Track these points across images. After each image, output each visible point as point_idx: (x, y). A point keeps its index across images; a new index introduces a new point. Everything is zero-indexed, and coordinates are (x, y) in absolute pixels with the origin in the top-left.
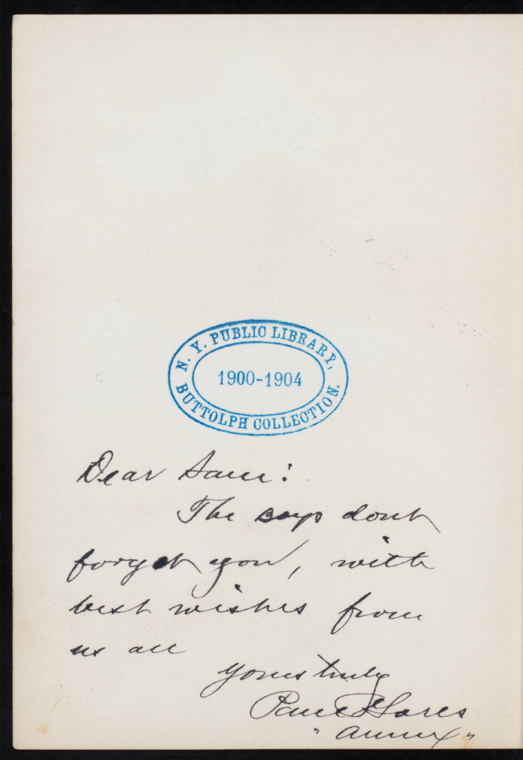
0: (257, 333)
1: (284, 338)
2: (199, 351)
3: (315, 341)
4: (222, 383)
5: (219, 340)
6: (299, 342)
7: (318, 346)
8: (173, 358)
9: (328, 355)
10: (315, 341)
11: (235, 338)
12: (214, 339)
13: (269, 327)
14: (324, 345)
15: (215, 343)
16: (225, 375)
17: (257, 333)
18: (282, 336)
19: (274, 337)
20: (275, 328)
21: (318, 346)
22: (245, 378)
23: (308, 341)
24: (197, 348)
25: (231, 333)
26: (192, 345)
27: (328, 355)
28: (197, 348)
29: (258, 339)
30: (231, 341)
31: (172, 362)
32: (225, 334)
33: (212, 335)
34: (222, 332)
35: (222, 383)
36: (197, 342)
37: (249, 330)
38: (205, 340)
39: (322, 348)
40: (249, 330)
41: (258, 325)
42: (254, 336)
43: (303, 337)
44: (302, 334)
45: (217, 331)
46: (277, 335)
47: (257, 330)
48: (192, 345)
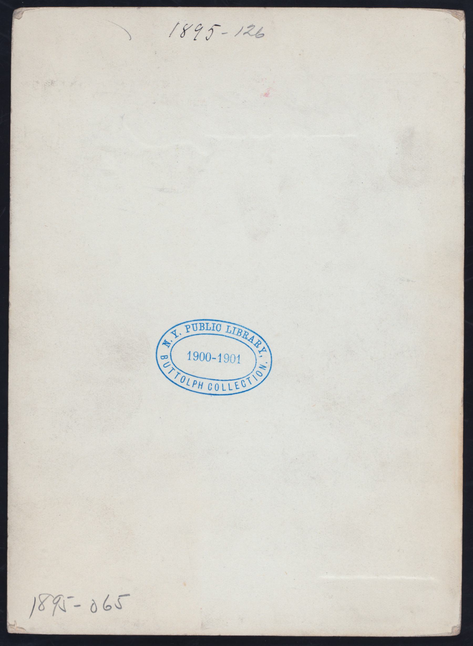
0: (215, 329)
1: (233, 333)
2: (176, 337)
3: (253, 337)
4: (189, 359)
5: (191, 330)
6: (243, 337)
7: (255, 341)
8: (162, 338)
9: (261, 348)
10: (253, 337)
11: (201, 330)
12: (187, 329)
13: (224, 326)
14: (259, 341)
15: (188, 332)
16: (192, 354)
17: (215, 329)
18: (232, 332)
19: (227, 332)
20: (228, 326)
21: (255, 341)
22: (205, 357)
23: (249, 337)
24: (175, 334)
25: (199, 326)
26: (172, 333)
27: (261, 348)
28: (175, 334)
29: (215, 332)
30: (198, 332)
31: (160, 340)
32: (195, 326)
33: (186, 326)
34: (193, 325)
35: (189, 359)
36: (175, 331)
37: (211, 325)
38: (181, 330)
39: (257, 343)
40: (211, 325)
41: (217, 323)
42: (213, 330)
43: (246, 335)
44: (246, 332)
45: (190, 324)
46: (229, 331)
47: (215, 326)
48: (172, 333)
